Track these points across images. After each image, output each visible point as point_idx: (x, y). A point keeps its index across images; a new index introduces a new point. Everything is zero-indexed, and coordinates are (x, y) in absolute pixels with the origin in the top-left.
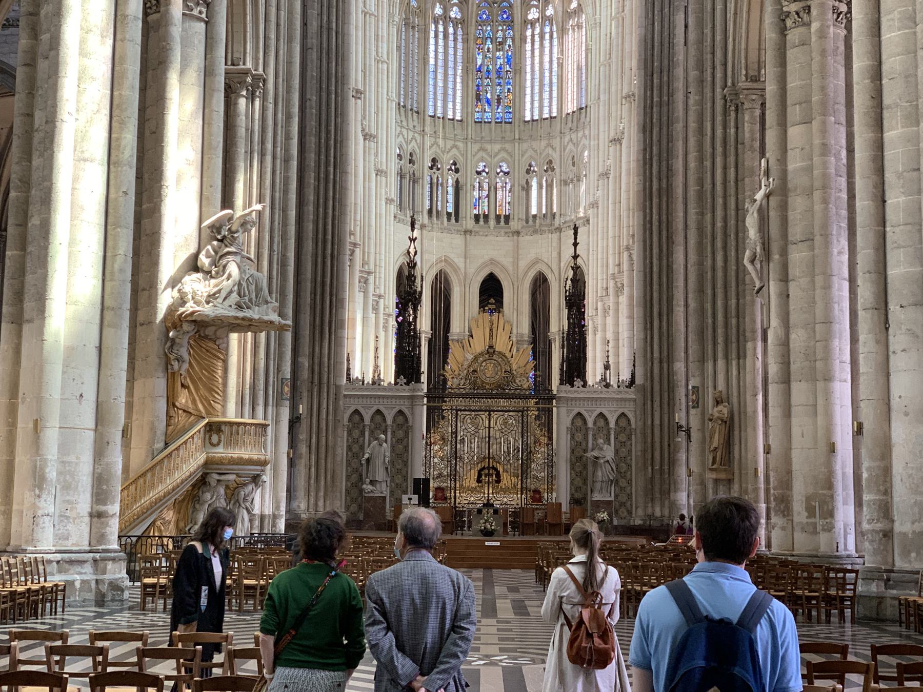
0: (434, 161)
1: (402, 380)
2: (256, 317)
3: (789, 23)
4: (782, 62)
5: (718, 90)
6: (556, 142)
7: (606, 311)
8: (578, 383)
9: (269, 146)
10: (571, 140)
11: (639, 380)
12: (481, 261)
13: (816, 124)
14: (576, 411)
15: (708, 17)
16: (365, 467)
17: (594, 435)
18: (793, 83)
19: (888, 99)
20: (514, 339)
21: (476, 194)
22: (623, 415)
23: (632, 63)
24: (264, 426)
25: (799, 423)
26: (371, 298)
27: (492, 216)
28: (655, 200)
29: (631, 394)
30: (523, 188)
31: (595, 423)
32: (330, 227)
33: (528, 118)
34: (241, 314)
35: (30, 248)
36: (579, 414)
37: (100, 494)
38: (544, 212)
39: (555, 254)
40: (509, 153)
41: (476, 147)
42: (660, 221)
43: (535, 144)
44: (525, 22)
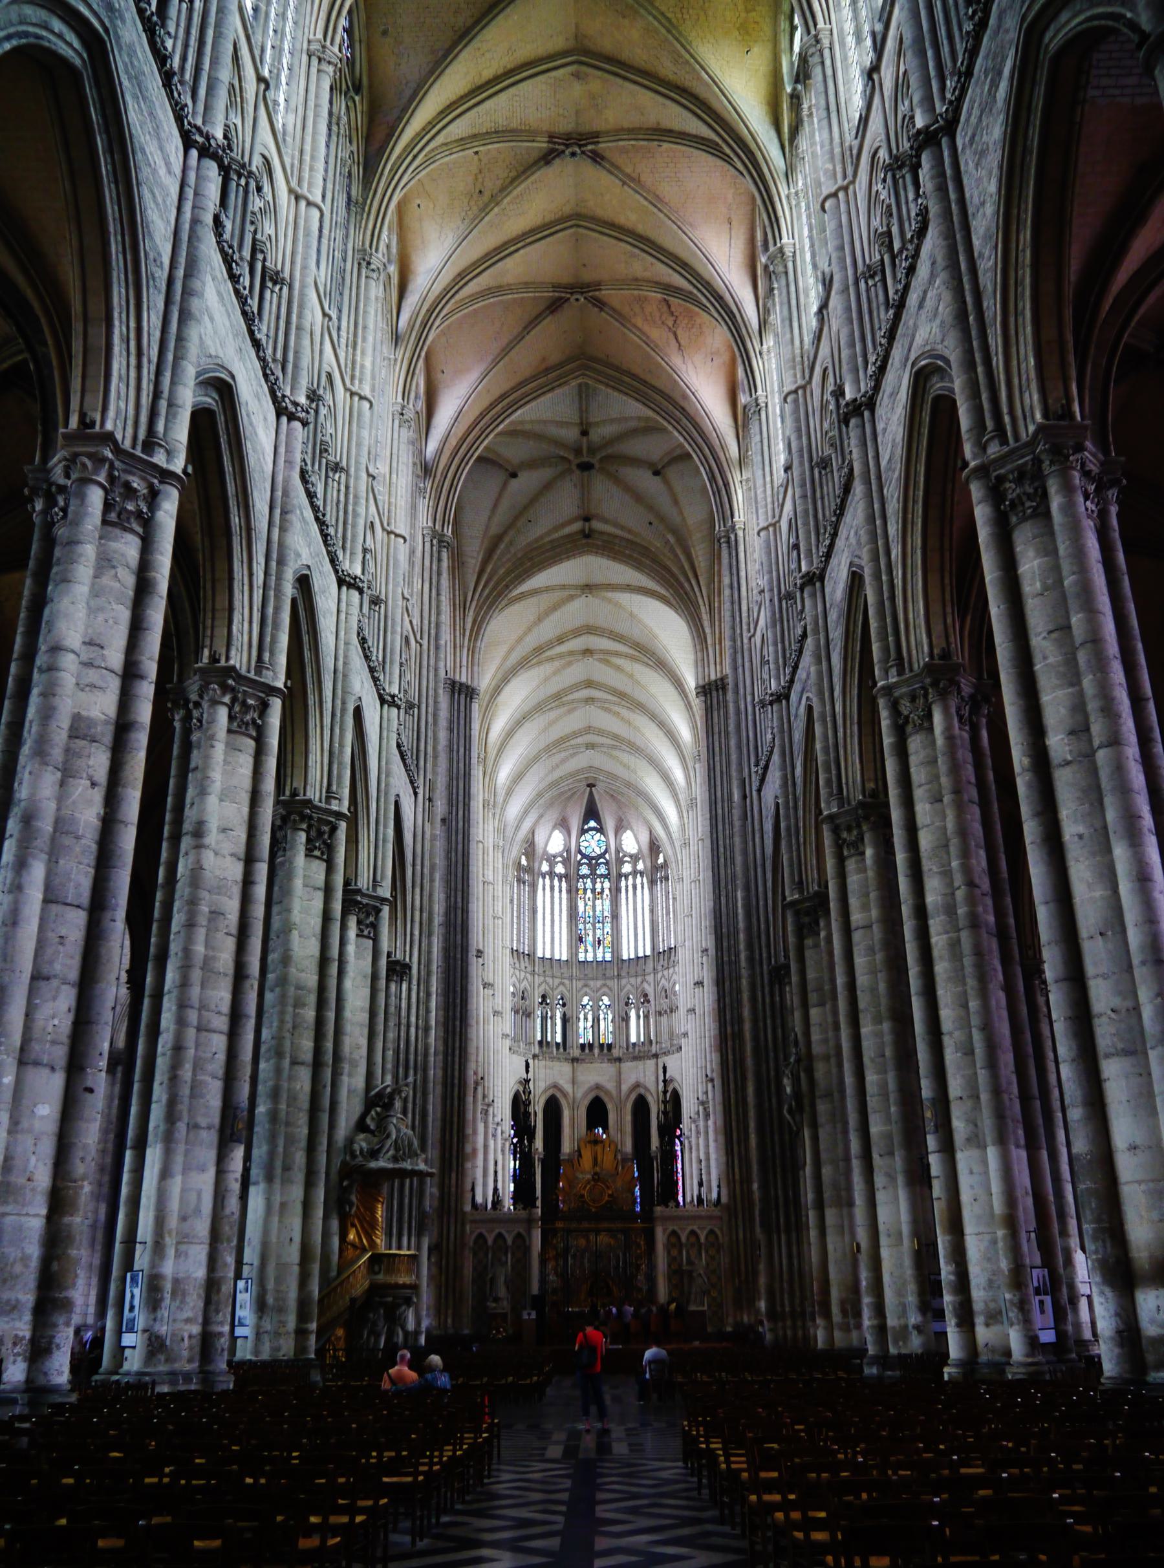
0: (544, 997)
1: (520, 1207)
2: (409, 1167)
3: (805, 931)
4: (801, 960)
5: (765, 967)
6: (650, 978)
7: (698, 1133)
8: (672, 1204)
9: (413, 1019)
10: (663, 976)
11: (724, 1200)
12: (586, 1087)
13: (828, 1006)
14: (671, 1228)
15: (754, 912)
16: (488, 1286)
17: (688, 1253)
18: (811, 975)
19: (862, 1005)
20: (619, 1157)
21: (581, 1024)
22: (712, 1232)
23: (707, 923)
24: (414, 1258)
25: (833, 1242)
26: (491, 1126)
27: (596, 1044)
28: (730, 1043)
29: (717, 1212)
30: (623, 1019)
31: (688, 1239)
32: (457, 1074)
33: (625, 957)
34: (397, 1166)
35: (256, 1129)
36: (674, 1233)
37: (303, 1316)
38: (642, 1039)
39: (653, 1078)
40: (611, 989)
41: (580, 984)
42: (734, 1061)
43: (632, 980)
44: (620, 876)
